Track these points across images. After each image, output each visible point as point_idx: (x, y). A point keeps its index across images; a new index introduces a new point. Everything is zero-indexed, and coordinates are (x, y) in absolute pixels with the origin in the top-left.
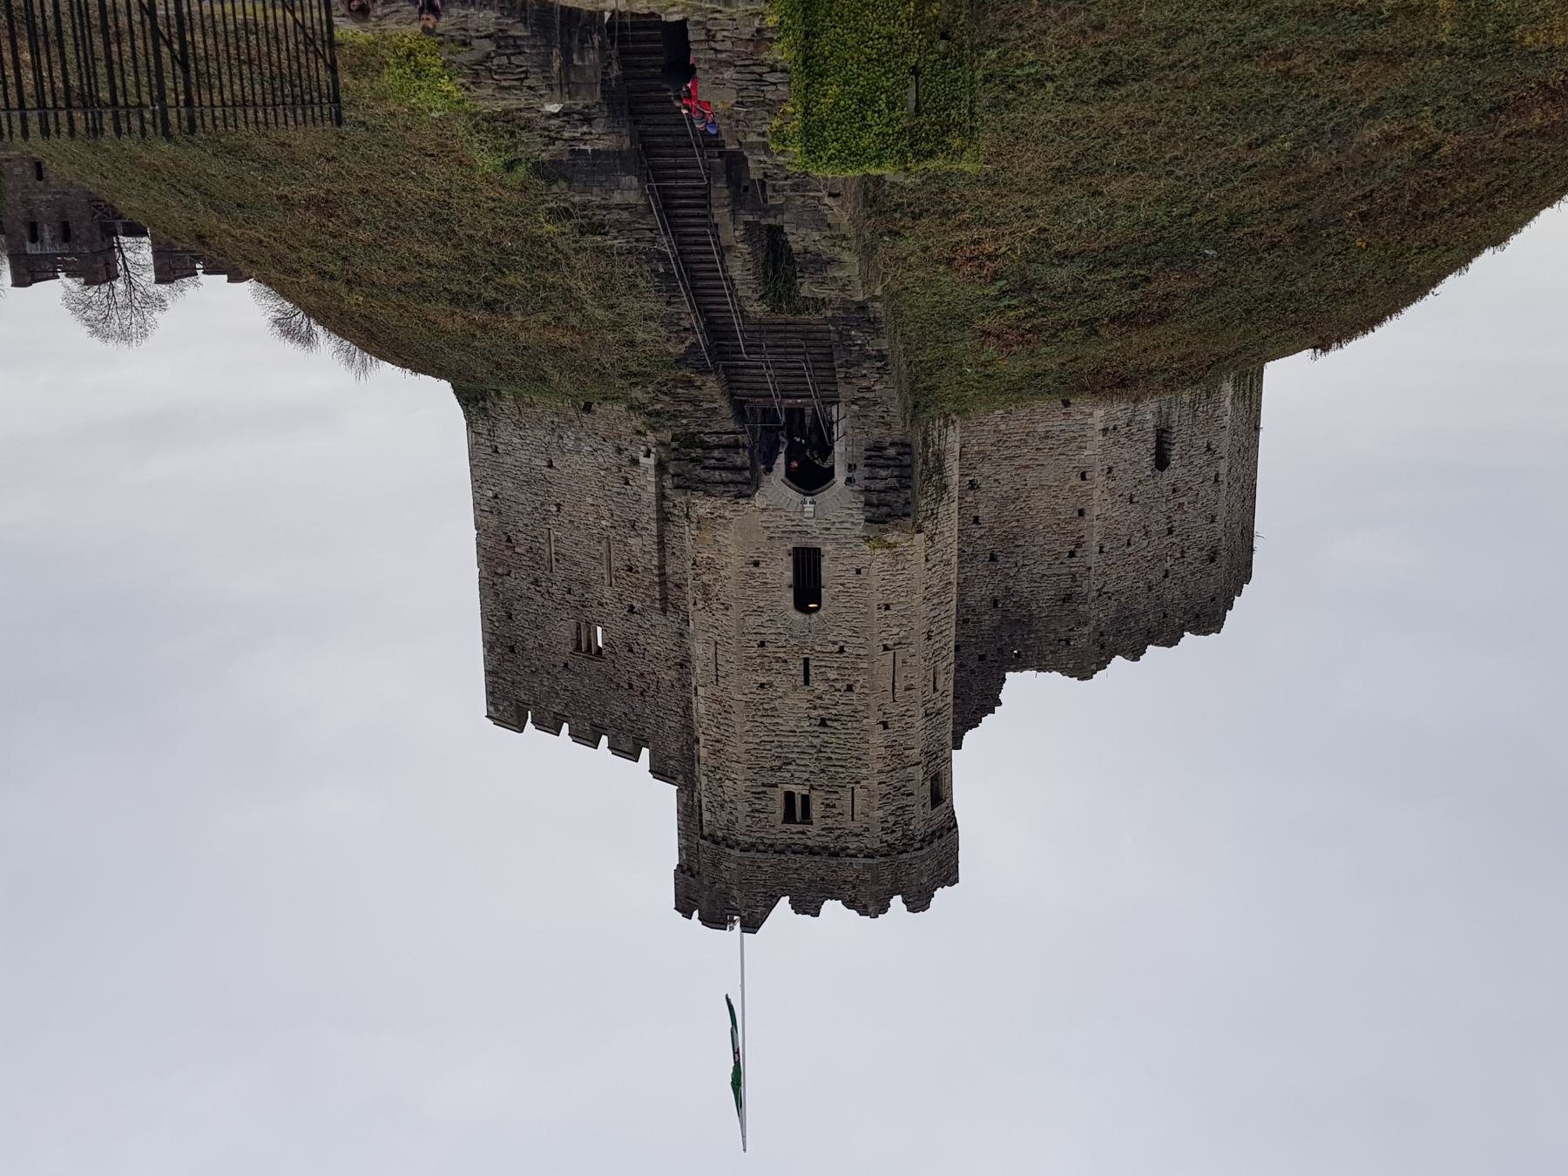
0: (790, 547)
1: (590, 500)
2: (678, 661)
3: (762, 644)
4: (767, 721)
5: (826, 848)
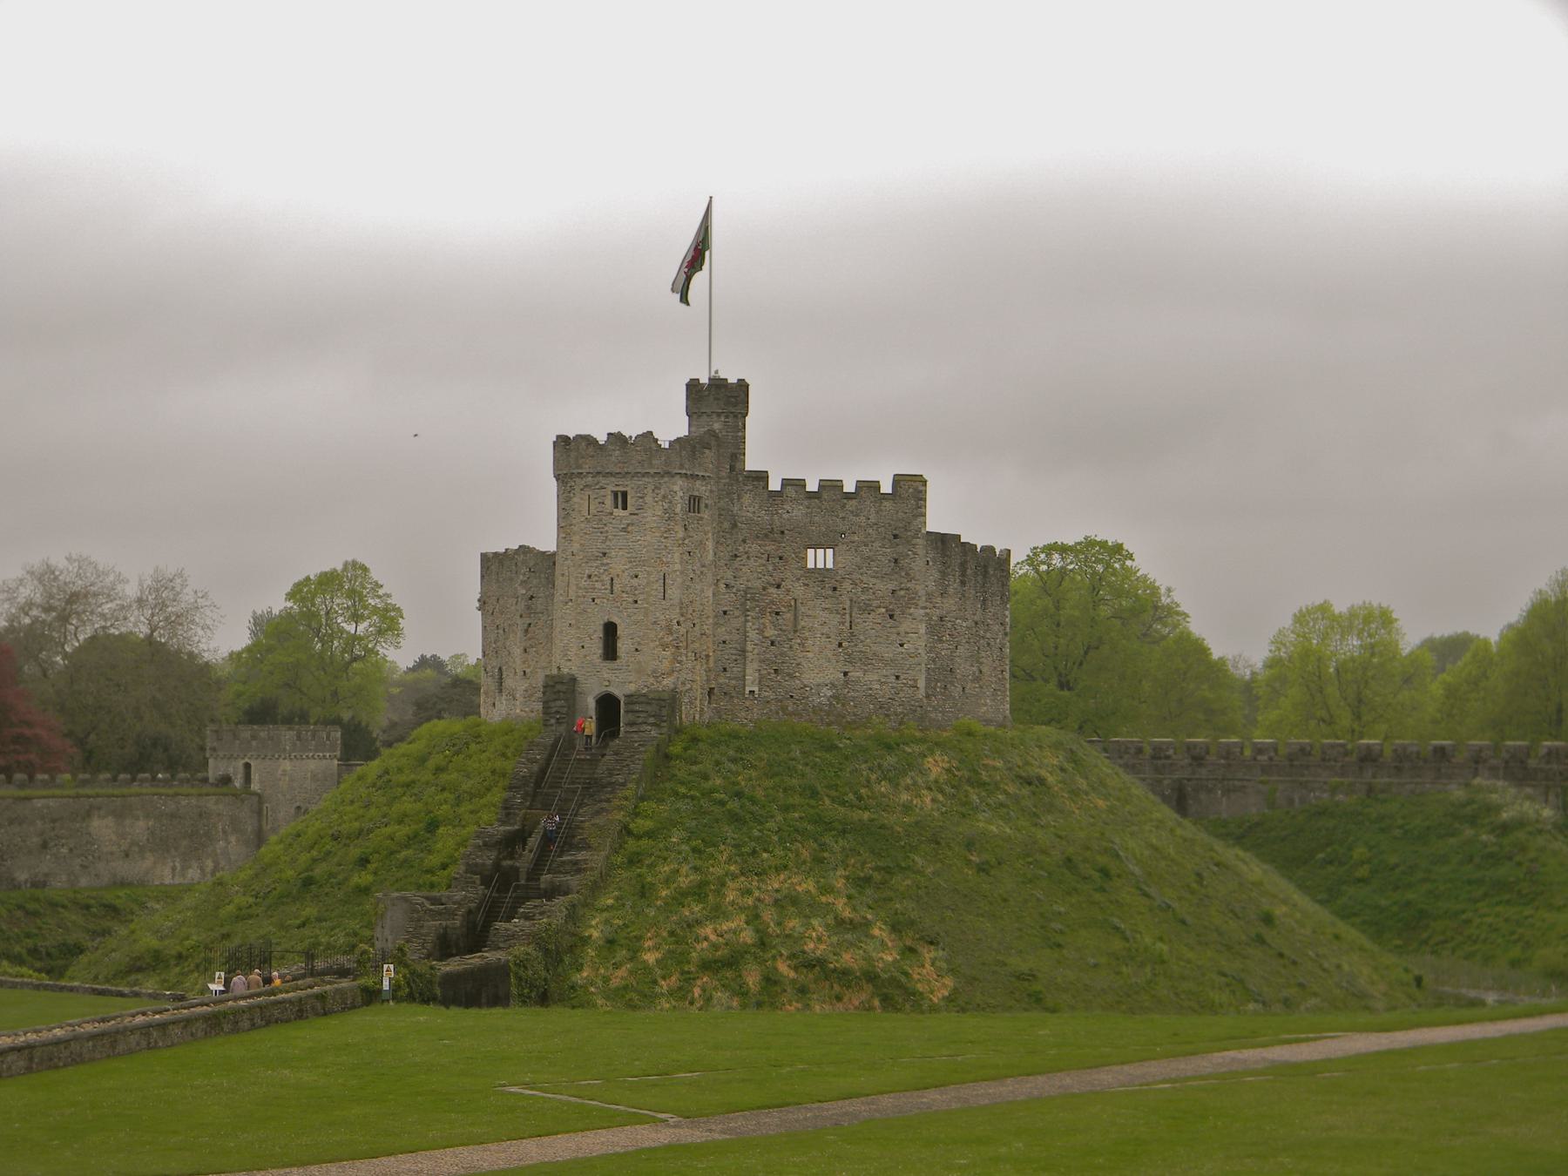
0: (618, 661)
1: (810, 655)
2: (738, 559)
3: (636, 602)
4: (634, 555)
5: (603, 476)
